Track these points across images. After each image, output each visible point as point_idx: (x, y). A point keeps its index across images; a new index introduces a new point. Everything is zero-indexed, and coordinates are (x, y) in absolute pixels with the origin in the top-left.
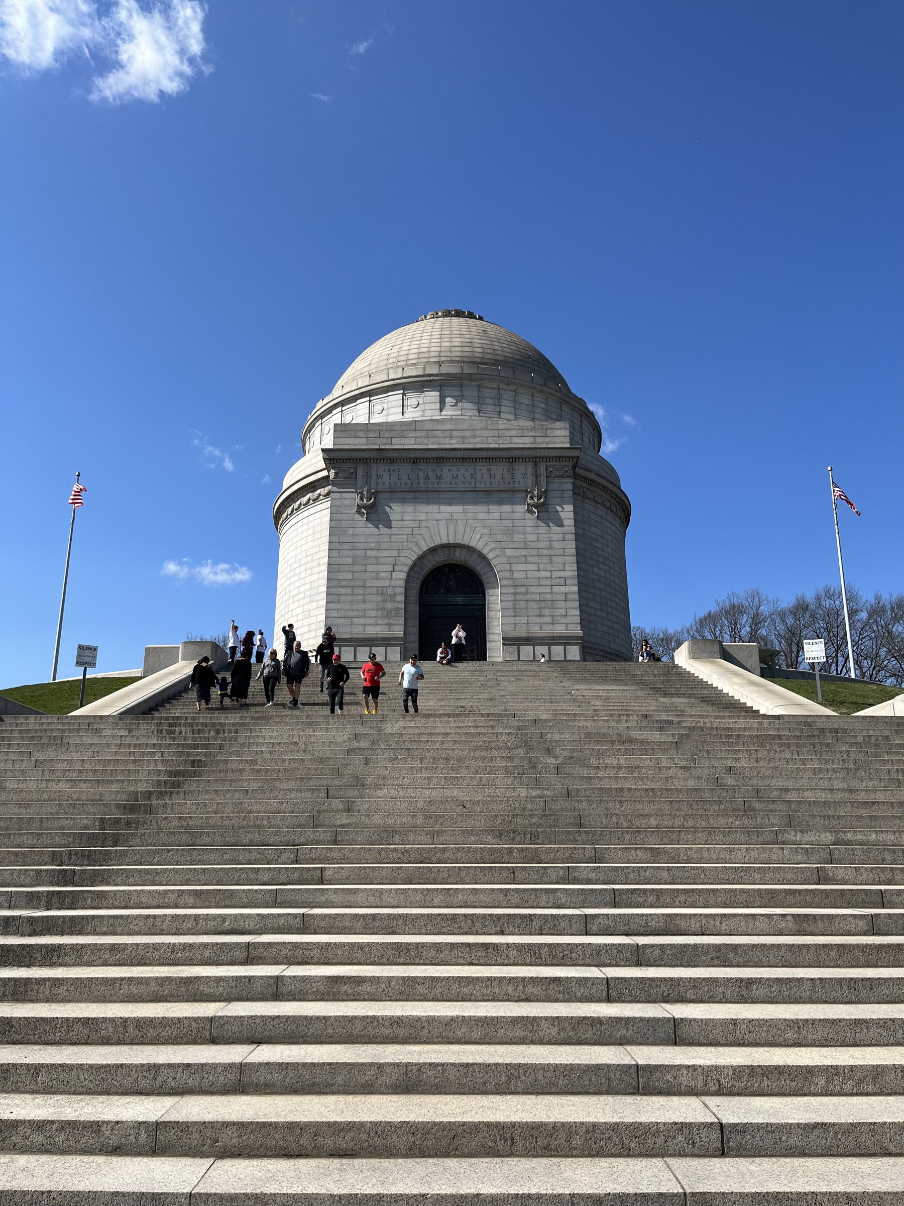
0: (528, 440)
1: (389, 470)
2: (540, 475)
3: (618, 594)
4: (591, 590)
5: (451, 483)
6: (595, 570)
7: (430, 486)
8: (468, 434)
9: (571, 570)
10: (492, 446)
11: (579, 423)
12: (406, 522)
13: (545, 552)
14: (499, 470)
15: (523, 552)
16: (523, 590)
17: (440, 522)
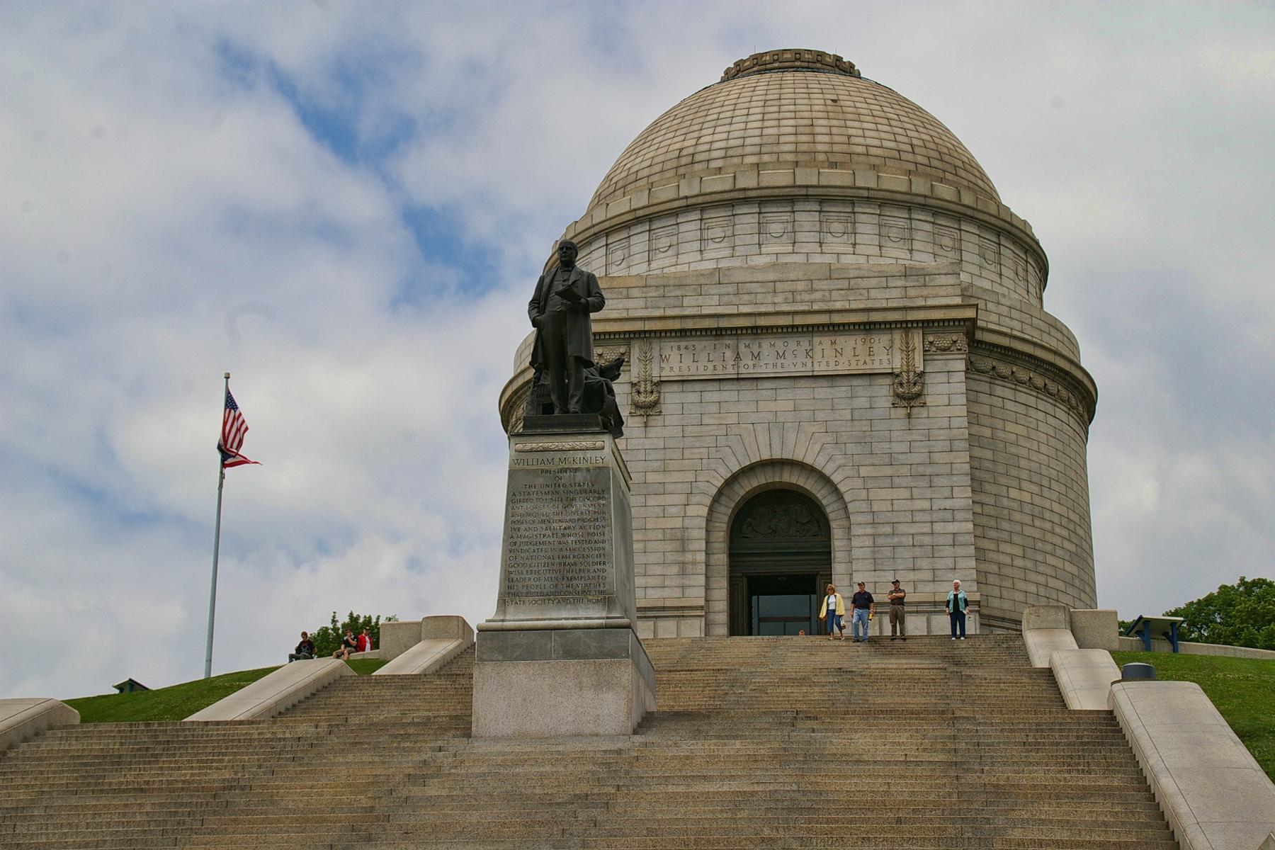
0: (896, 293)
1: (679, 348)
2: (913, 350)
3: (1057, 530)
4: (1006, 525)
5: (775, 366)
6: (1014, 493)
7: (742, 370)
8: (801, 286)
9: (963, 498)
10: (838, 305)
11: (995, 247)
12: (706, 428)
13: (921, 469)
14: (848, 343)
15: (888, 471)
16: (888, 529)
17: (759, 427)
